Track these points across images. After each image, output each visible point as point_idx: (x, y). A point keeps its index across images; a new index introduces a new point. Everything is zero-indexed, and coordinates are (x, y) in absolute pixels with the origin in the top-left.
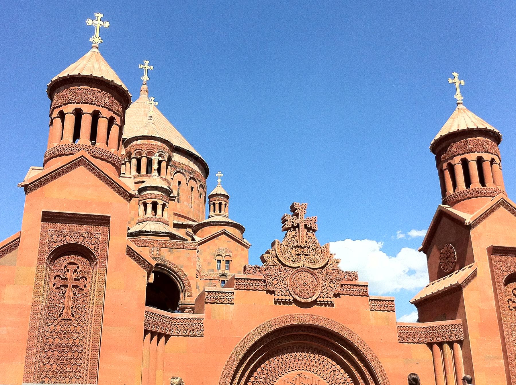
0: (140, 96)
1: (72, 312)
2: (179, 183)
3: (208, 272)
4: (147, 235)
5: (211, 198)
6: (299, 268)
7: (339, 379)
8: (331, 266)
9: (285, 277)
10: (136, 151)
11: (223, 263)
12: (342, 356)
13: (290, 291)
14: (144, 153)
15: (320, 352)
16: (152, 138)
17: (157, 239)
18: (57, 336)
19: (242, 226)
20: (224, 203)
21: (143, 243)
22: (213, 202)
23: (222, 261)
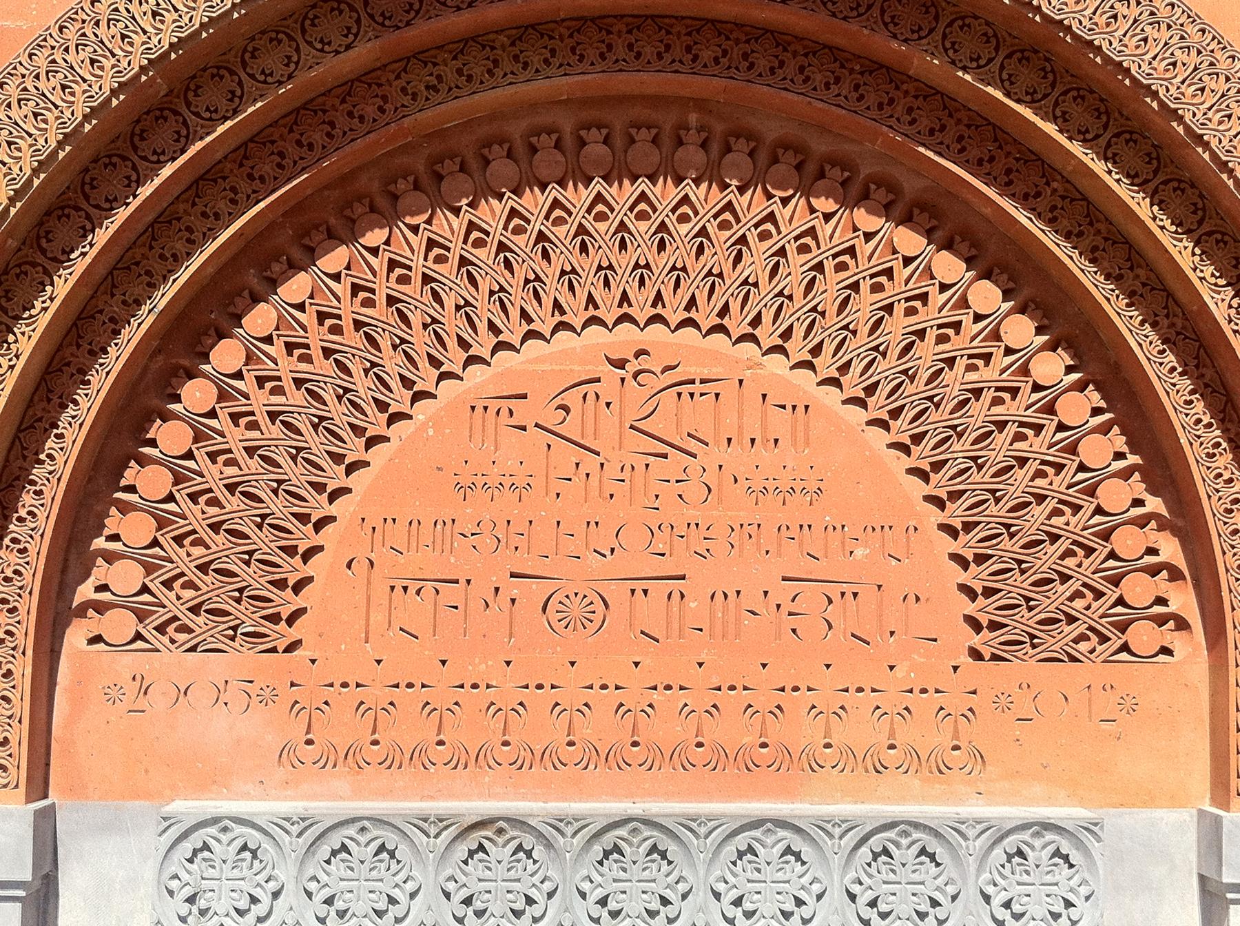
7: (987, 396)
12: (1024, 200)
15: (821, 175)
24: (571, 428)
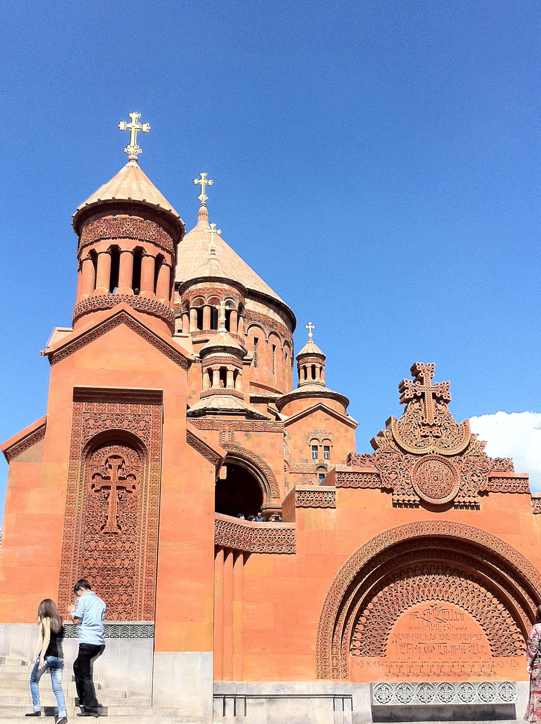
0: (199, 222)
1: (118, 522)
2: (256, 340)
3: (300, 463)
4: (215, 414)
5: (300, 359)
6: (426, 456)
7: (491, 612)
8: (474, 451)
9: (407, 469)
10: (196, 299)
11: (321, 450)
12: (494, 579)
13: (415, 488)
14: (206, 301)
15: (461, 574)
16: (217, 279)
17: (229, 420)
18: (100, 555)
19: (345, 398)
20: (318, 366)
21: (210, 425)
22: (304, 365)
23: (319, 447)
24: (425, 617)
